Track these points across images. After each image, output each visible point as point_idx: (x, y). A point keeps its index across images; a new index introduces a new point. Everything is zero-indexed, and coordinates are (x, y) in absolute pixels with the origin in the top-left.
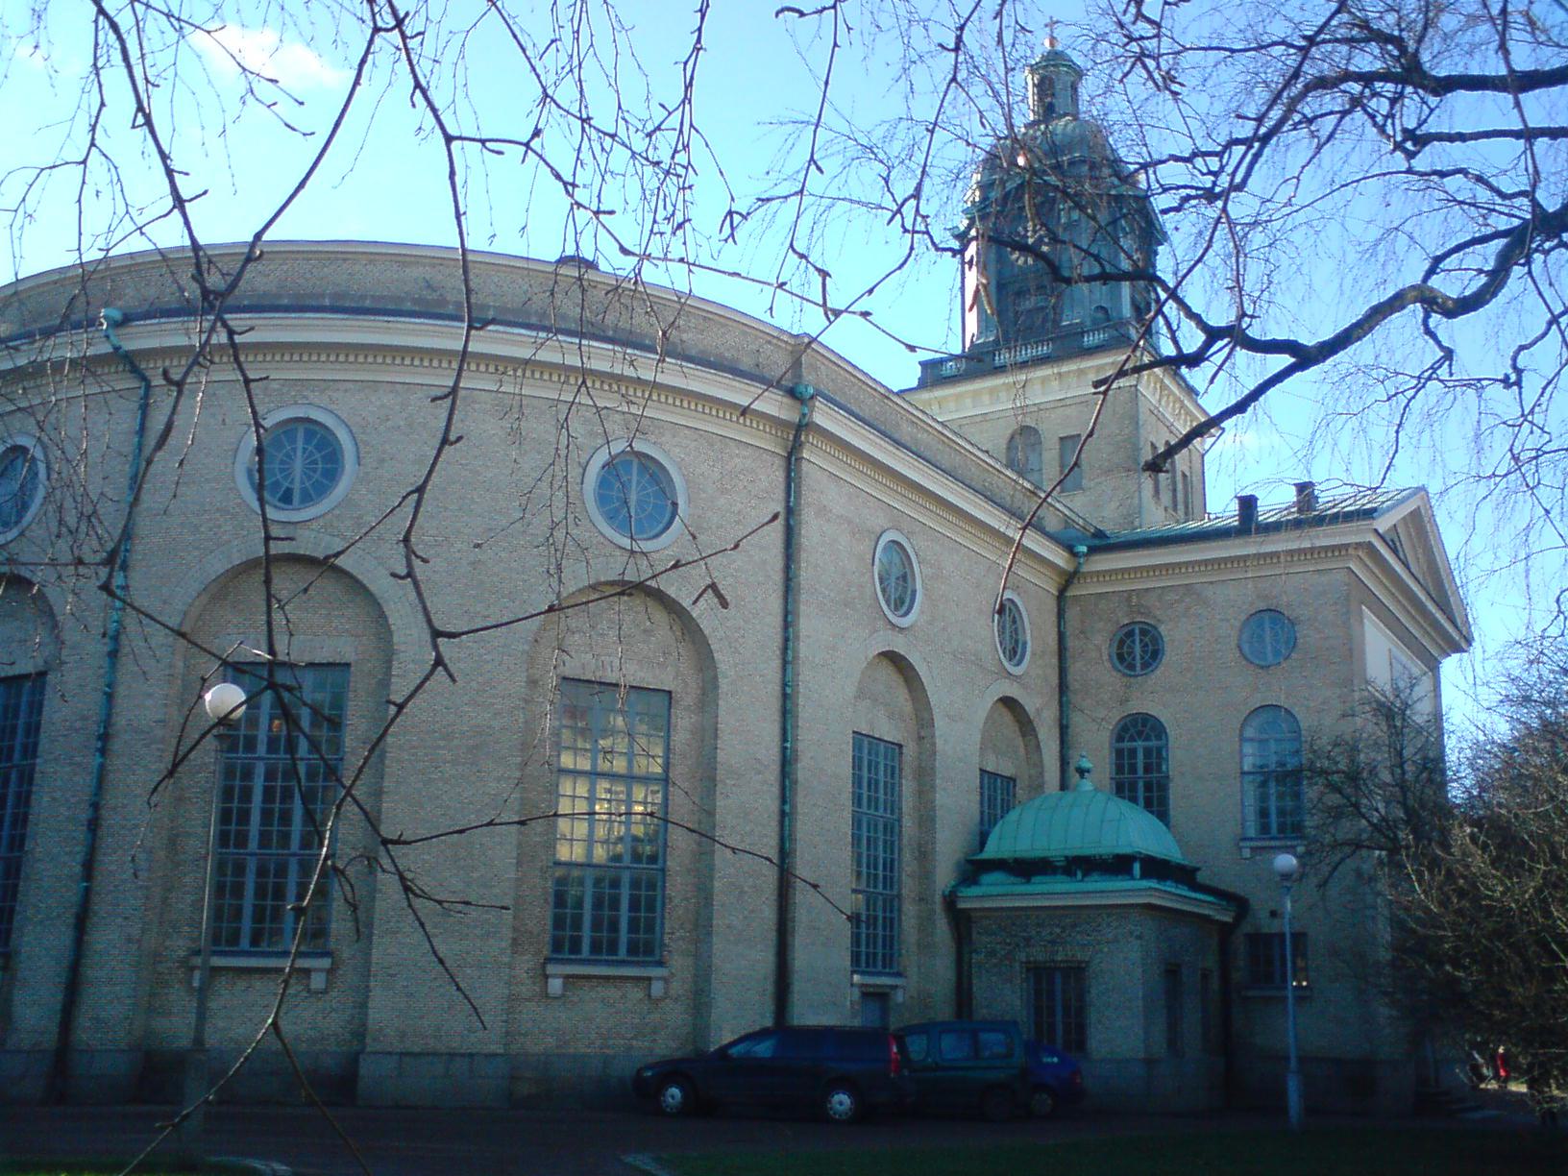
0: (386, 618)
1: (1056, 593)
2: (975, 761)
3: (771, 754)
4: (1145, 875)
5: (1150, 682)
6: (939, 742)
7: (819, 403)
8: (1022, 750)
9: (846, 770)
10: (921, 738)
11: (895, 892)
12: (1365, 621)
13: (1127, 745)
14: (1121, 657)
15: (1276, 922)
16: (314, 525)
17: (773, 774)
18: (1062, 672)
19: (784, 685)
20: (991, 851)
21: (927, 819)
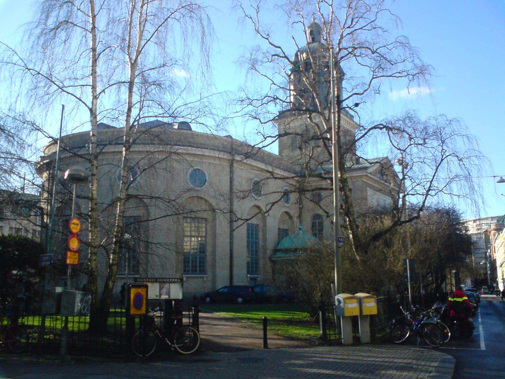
7: (236, 155)
8: (290, 223)
21: (265, 240)
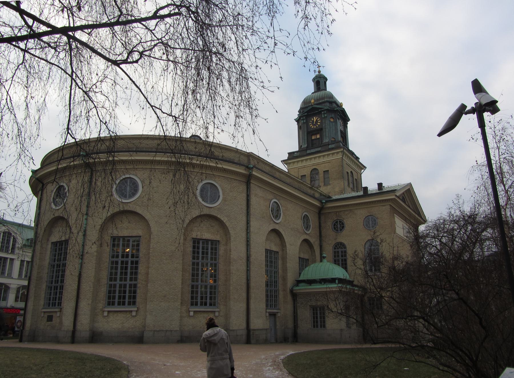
0: (149, 225)
1: (318, 212)
2: (298, 256)
3: (244, 255)
4: (339, 283)
6: (288, 251)
8: (310, 252)
9: (263, 258)
10: (283, 250)
12: (396, 218)
13: (336, 250)
14: (335, 228)
16: (132, 203)
17: (244, 260)
19: (247, 238)
20: (301, 278)
21: (285, 270)
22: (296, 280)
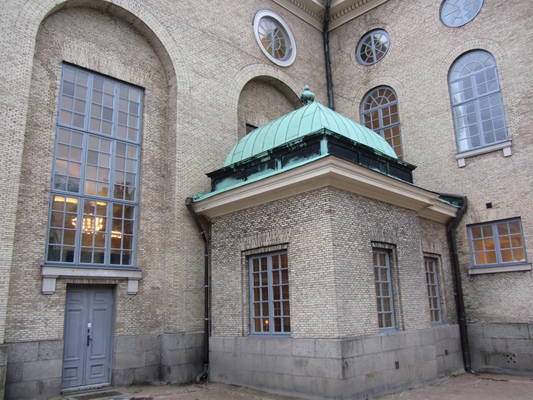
1: (322, 31)
5: (382, 65)
11: (135, 201)
14: (364, 57)
15: (492, 211)
18: (329, 77)
22: (209, 175)
